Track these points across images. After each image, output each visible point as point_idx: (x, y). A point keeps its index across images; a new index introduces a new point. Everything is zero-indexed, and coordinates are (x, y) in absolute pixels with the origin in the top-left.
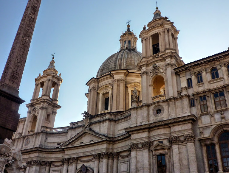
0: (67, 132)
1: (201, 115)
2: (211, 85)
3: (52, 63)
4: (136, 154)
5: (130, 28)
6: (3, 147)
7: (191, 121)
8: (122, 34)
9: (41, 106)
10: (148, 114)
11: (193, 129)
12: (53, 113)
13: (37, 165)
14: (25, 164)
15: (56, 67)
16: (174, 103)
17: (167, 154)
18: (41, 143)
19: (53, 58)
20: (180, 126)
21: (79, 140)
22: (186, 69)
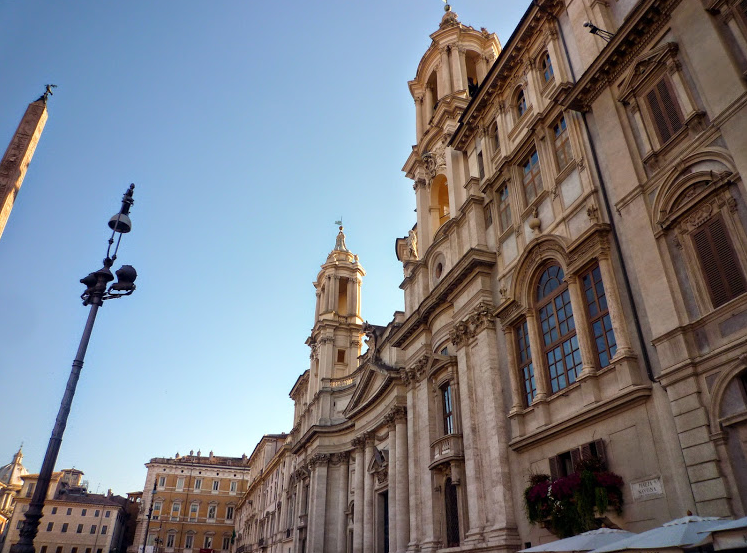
1: (502, 241)
3: (340, 239)
4: (414, 398)
7: (477, 270)
12: (351, 344)
13: (320, 466)
17: (453, 379)
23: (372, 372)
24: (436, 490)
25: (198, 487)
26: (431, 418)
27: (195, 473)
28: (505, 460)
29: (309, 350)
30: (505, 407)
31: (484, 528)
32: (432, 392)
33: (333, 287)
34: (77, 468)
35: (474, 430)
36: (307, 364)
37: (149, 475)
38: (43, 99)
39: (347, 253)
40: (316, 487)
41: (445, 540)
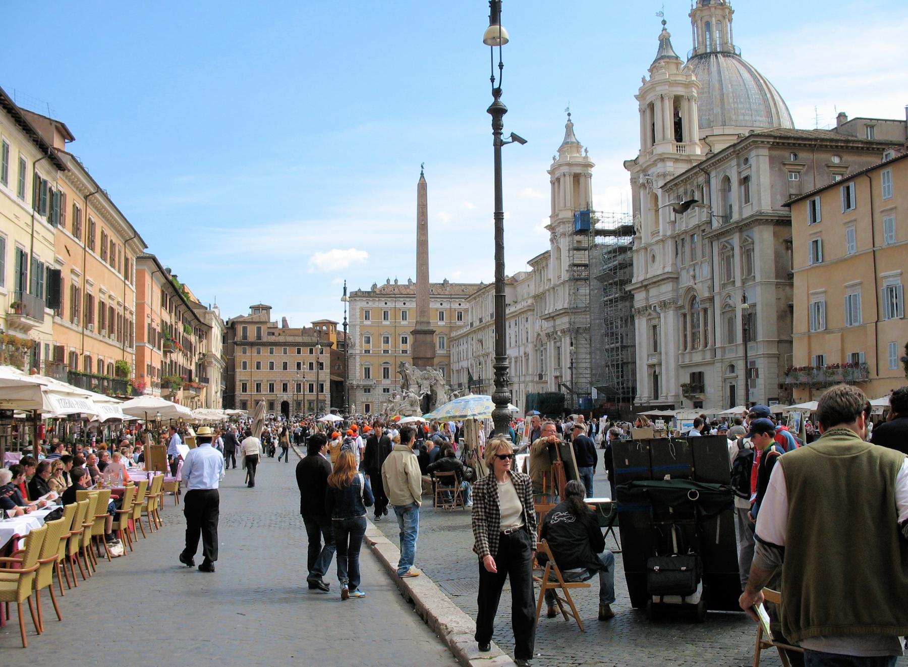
1: (681, 269)
3: (569, 128)
7: (670, 280)
8: (692, 6)
9: (561, 231)
11: (676, 290)
14: (559, 333)
15: (580, 135)
16: (664, 248)
19: (569, 115)
20: (665, 285)
22: (671, 189)
24: (649, 375)
25: (404, 318)
26: (648, 339)
27: (400, 305)
29: (548, 234)
30: (679, 349)
31: (668, 394)
33: (568, 182)
34: (266, 303)
35: (666, 353)
36: (547, 246)
38: (422, 174)
39: (577, 146)
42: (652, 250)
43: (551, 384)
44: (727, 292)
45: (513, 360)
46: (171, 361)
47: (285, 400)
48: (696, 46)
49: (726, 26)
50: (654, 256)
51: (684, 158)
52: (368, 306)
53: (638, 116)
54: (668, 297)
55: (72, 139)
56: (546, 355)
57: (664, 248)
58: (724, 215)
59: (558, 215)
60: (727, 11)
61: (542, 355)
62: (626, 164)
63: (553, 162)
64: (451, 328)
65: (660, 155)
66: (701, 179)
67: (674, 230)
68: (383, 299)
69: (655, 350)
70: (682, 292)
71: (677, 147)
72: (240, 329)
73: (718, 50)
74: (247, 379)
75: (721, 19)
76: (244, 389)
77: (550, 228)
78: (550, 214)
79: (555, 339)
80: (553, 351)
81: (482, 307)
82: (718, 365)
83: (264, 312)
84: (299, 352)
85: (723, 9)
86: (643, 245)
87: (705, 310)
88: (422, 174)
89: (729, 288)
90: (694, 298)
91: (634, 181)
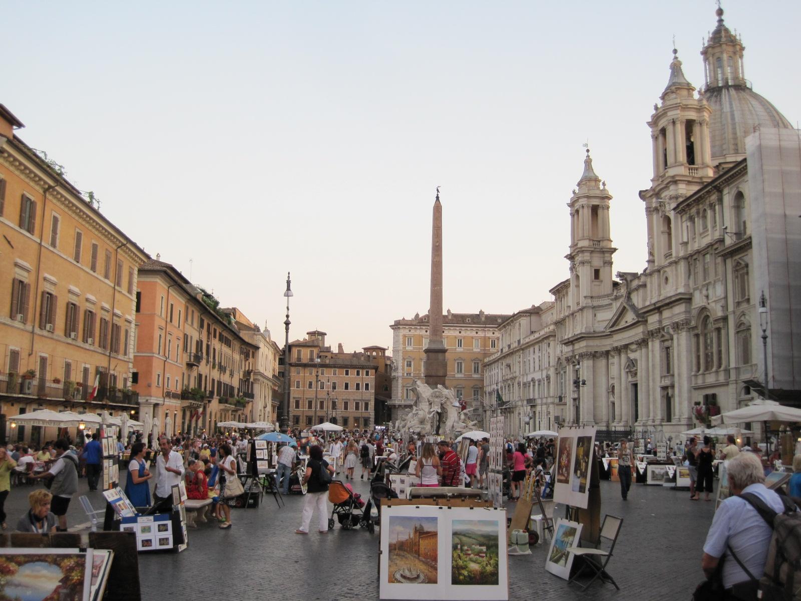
0: (611, 304)
1: (695, 289)
2: (703, 239)
3: (588, 162)
5: (723, 17)
6: (436, 391)
7: (683, 301)
8: (704, 44)
10: (659, 286)
11: (688, 312)
13: (588, 359)
16: (676, 268)
18: (587, 324)
19: (588, 151)
21: (623, 318)
22: (683, 210)
23: (624, 308)
26: (661, 360)
28: (690, 391)
29: (568, 263)
30: (691, 370)
32: (661, 348)
33: (586, 213)
34: (320, 330)
37: (396, 337)
38: (438, 198)
39: (597, 180)
40: (585, 373)
41: (666, 418)
42: (665, 272)
43: (569, 406)
44: (741, 310)
45: (537, 383)
46: (200, 376)
47: (334, 416)
48: (708, 81)
49: (738, 61)
50: (667, 279)
51: (694, 180)
52: (410, 333)
53: (650, 142)
54: (683, 317)
55: (20, 125)
56: (565, 378)
57: (676, 270)
58: (738, 232)
59: (577, 245)
60: (738, 47)
61: (562, 379)
62: (642, 195)
63: (572, 195)
64: (486, 355)
65: (673, 177)
66: (714, 197)
67: (686, 250)
68: (424, 327)
69: (668, 371)
70: (694, 313)
71: (689, 170)
72: (295, 351)
73: (730, 84)
74: (300, 396)
75: (731, 54)
76: (297, 406)
77: (571, 257)
78: (570, 243)
79: (574, 362)
80: (571, 375)
81: (510, 335)
82: (732, 388)
83: (320, 337)
84: (347, 374)
85: (734, 46)
86: (656, 268)
87: (718, 330)
88: (438, 198)
89: (744, 306)
90: (707, 317)
91: (650, 211)
